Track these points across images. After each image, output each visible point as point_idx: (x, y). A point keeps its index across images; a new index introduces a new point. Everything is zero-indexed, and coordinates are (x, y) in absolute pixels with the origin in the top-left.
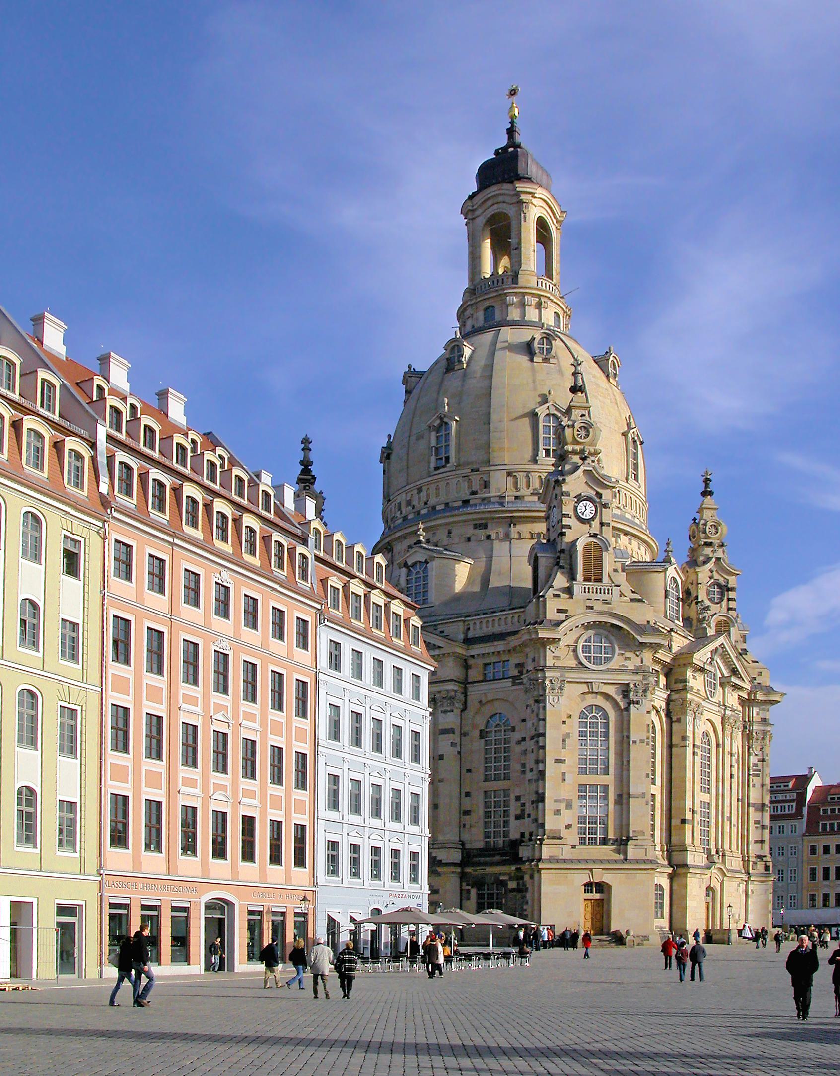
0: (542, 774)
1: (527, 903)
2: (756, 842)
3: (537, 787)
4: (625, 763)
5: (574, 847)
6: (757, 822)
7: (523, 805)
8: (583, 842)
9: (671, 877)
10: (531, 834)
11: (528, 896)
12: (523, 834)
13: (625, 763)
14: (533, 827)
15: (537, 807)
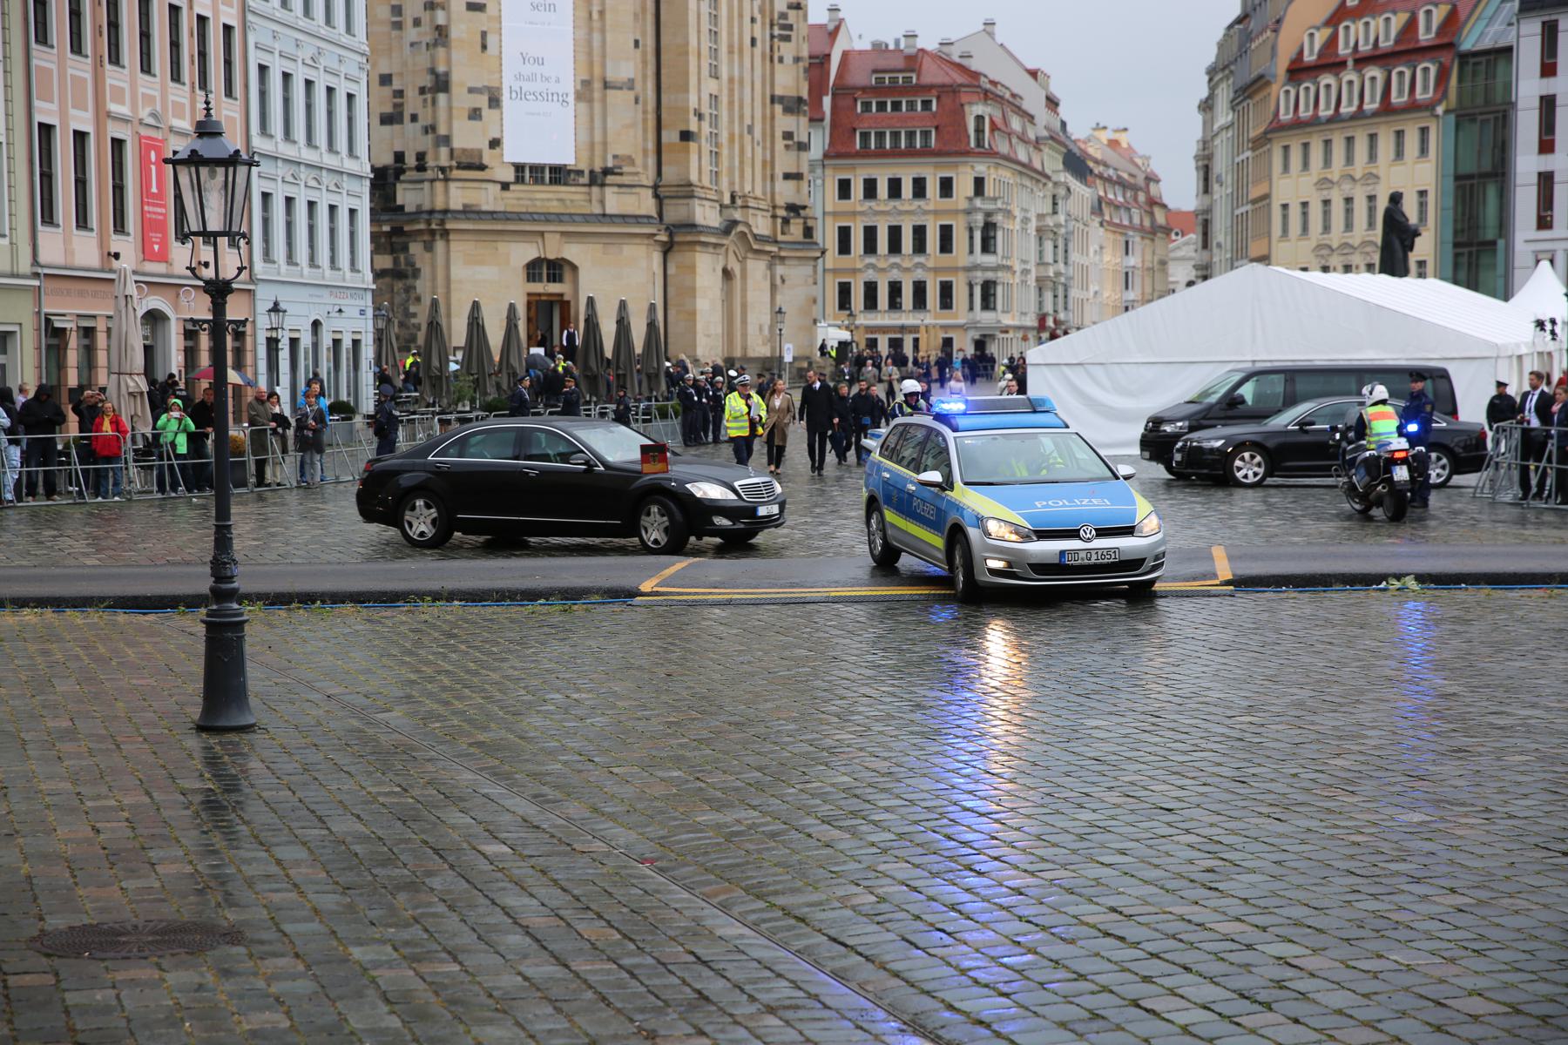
0: (442, 33)
1: (418, 299)
2: (787, 176)
3: (433, 59)
4: (595, 16)
5: (505, 186)
6: (788, 135)
7: (399, 93)
8: (519, 180)
9: (667, 249)
10: (421, 157)
11: (422, 286)
12: (399, 157)
13: (595, 16)
14: (426, 143)
15: (434, 102)
